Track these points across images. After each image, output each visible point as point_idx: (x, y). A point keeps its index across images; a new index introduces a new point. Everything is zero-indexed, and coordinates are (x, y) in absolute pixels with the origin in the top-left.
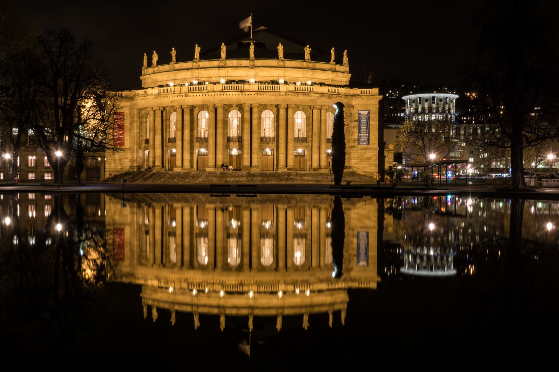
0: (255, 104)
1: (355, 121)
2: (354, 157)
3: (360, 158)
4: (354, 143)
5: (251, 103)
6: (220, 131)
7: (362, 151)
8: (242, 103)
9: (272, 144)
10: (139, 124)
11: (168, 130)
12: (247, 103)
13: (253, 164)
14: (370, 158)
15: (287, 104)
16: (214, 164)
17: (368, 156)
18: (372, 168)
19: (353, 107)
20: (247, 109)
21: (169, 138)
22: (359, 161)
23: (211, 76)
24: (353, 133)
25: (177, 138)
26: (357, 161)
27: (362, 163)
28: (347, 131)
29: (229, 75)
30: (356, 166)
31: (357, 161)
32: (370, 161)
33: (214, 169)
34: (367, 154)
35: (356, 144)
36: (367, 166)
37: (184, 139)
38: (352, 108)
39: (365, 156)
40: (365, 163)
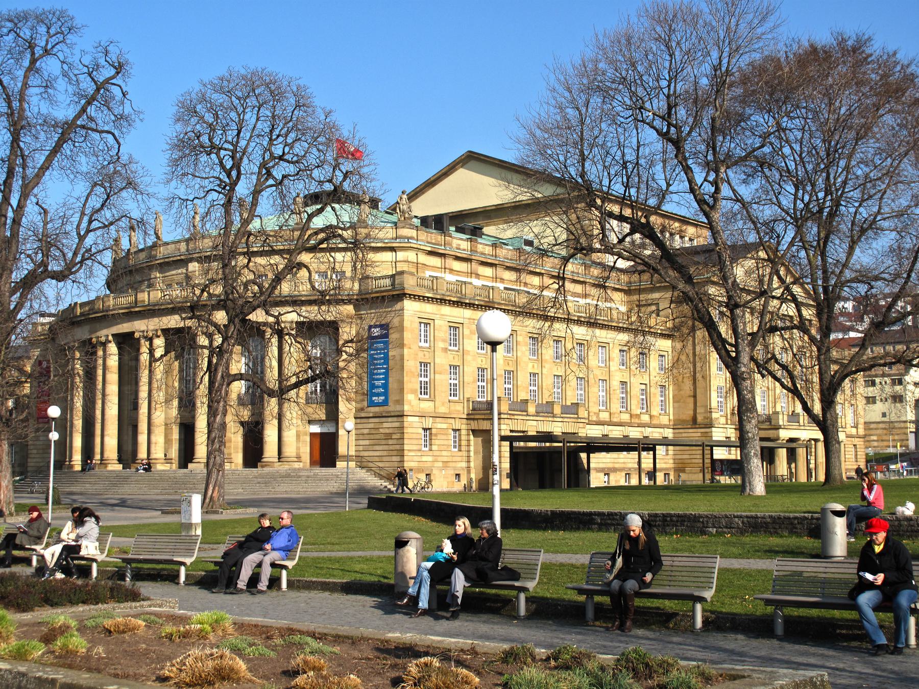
3: (372, 437)
4: (363, 400)
14: (388, 436)
17: (387, 431)
18: (394, 459)
22: (372, 442)
26: (367, 442)
27: (377, 448)
30: (366, 454)
31: (367, 442)
32: (390, 442)
34: (385, 425)
35: (365, 404)
36: (385, 453)
39: (381, 430)
40: (381, 448)
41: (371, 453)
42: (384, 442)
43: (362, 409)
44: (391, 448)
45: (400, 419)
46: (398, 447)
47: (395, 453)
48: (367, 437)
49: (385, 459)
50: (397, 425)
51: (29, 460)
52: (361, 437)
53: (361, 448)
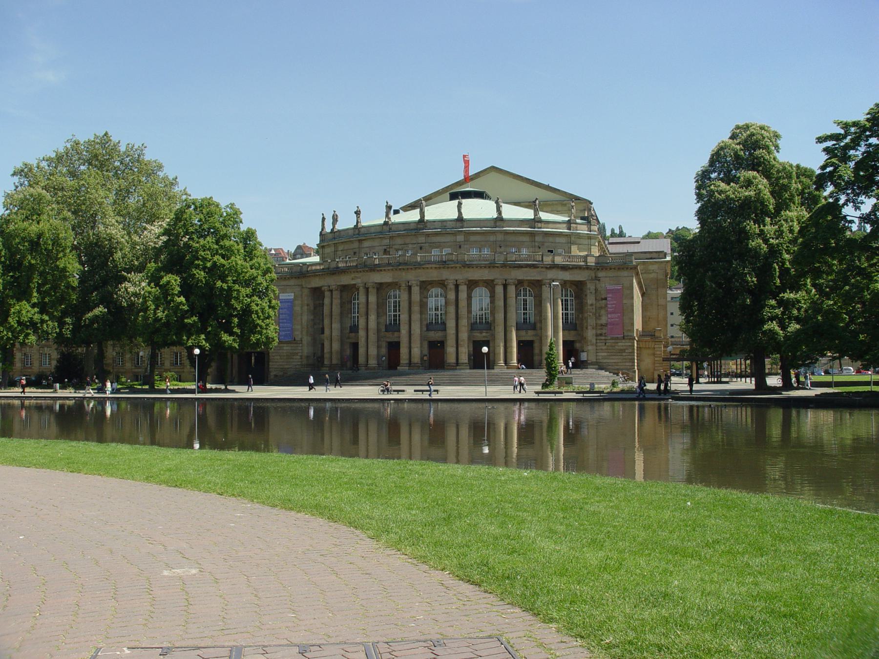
0: (461, 280)
1: (602, 299)
2: (602, 349)
5: (457, 278)
6: (416, 317)
7: (613, 341)
8: (444, 279)
9: (487, 333)
10: (312, 308)
11: (350, 315)
12: (452, 278)
13: (460, 361)
14: (623, 351)
15: (506, 278)
16: (407, 362)
17: (622, 348)
18: (627, 364)
19: (599, 280)
20: (451, 286)
21: (350, 327)
23: (407, 243)
24: (599, 316)
25: (360, 327)
26: (605, 354)
27: (613, 357)
28: (591, 314)
29: (429, 241)
30: (605, 361)
31: (605, 354)
32: (624, 354)
33: (407, 368)
34: (620, 344)
36: (620, 361)
37: (369, 327)
38: (597, 282)
39: (617, 347)
40: (617, 357)
41: (608, 361)
42: (619, 354)
43: (601, 335)
44: (625, 357)
45: (631, 341)
46: (630, 357)
47: (628, 361)
48: (606, 351)
49: (620, 364)
50: (630, 344)
51: (270, 363)
52: (600, 351)
53: (600, 358)
